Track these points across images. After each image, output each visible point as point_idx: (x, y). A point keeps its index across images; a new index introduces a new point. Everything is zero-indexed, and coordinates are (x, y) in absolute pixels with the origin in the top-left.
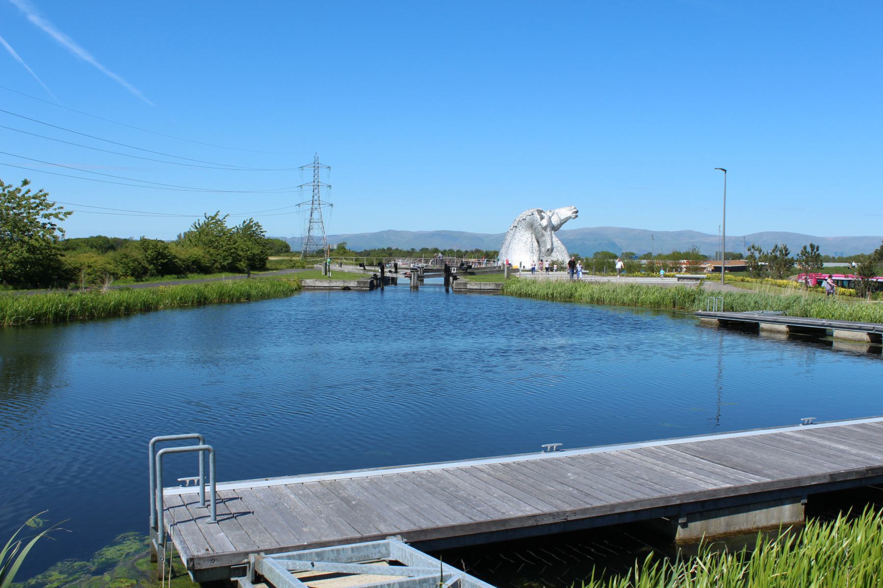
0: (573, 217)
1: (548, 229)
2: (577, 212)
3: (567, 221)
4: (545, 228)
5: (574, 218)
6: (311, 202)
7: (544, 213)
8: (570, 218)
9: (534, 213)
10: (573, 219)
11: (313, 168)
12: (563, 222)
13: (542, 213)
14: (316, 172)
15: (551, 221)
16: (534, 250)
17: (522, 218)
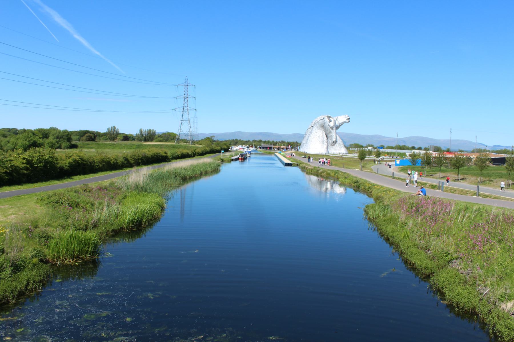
0: (347, 122)
1: (334, 128)
2: (349, 119)
3: (343, 124)
4: (332, 128)
5: (348, 123)
6: (183, 107)
7: (331, 118)
8: (345, 122)
9: (324, 118)
10: (347, 123)
11: (185, 86)
12: (341, 124)
13: (330, 118)
14: (186, 88)
15: (336, 124)
16: (324, 142)
17: (317, 121)
